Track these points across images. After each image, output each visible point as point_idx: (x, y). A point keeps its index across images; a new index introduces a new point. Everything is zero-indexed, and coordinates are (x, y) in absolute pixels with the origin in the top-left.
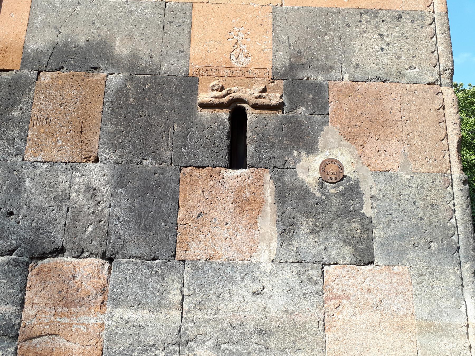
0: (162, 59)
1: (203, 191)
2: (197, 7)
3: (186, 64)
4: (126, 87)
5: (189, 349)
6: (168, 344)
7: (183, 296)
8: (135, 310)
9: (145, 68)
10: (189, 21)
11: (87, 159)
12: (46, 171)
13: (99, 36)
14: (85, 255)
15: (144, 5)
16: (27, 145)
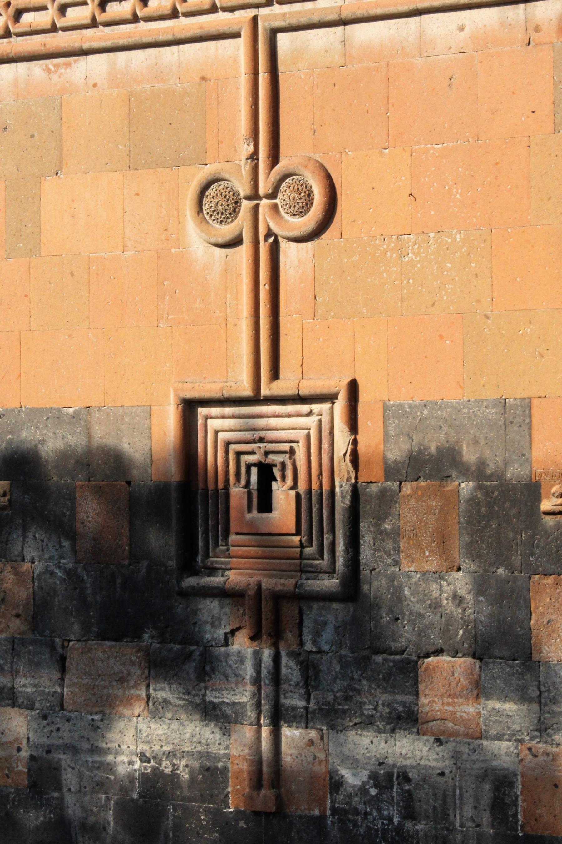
0: (506, 464)
1: (550, 599)
2: (535, 402)
3: (529, 468)
4: (476, 496)
5: (548, 734)
6: (531, 730)
7: (540, 692)
8: (503, 702)
9: (492, 475)
10: (527, 421)
11: (450, 569)
12: (419, 581)
13: (447, 442)
14: (460, 655)
15: (485, 404)
16: (401, 557)
